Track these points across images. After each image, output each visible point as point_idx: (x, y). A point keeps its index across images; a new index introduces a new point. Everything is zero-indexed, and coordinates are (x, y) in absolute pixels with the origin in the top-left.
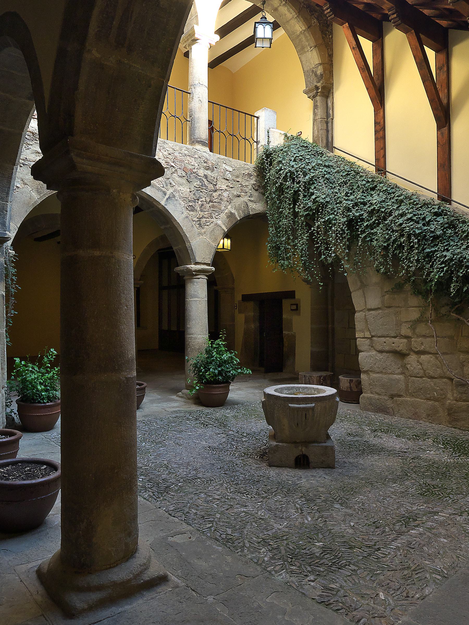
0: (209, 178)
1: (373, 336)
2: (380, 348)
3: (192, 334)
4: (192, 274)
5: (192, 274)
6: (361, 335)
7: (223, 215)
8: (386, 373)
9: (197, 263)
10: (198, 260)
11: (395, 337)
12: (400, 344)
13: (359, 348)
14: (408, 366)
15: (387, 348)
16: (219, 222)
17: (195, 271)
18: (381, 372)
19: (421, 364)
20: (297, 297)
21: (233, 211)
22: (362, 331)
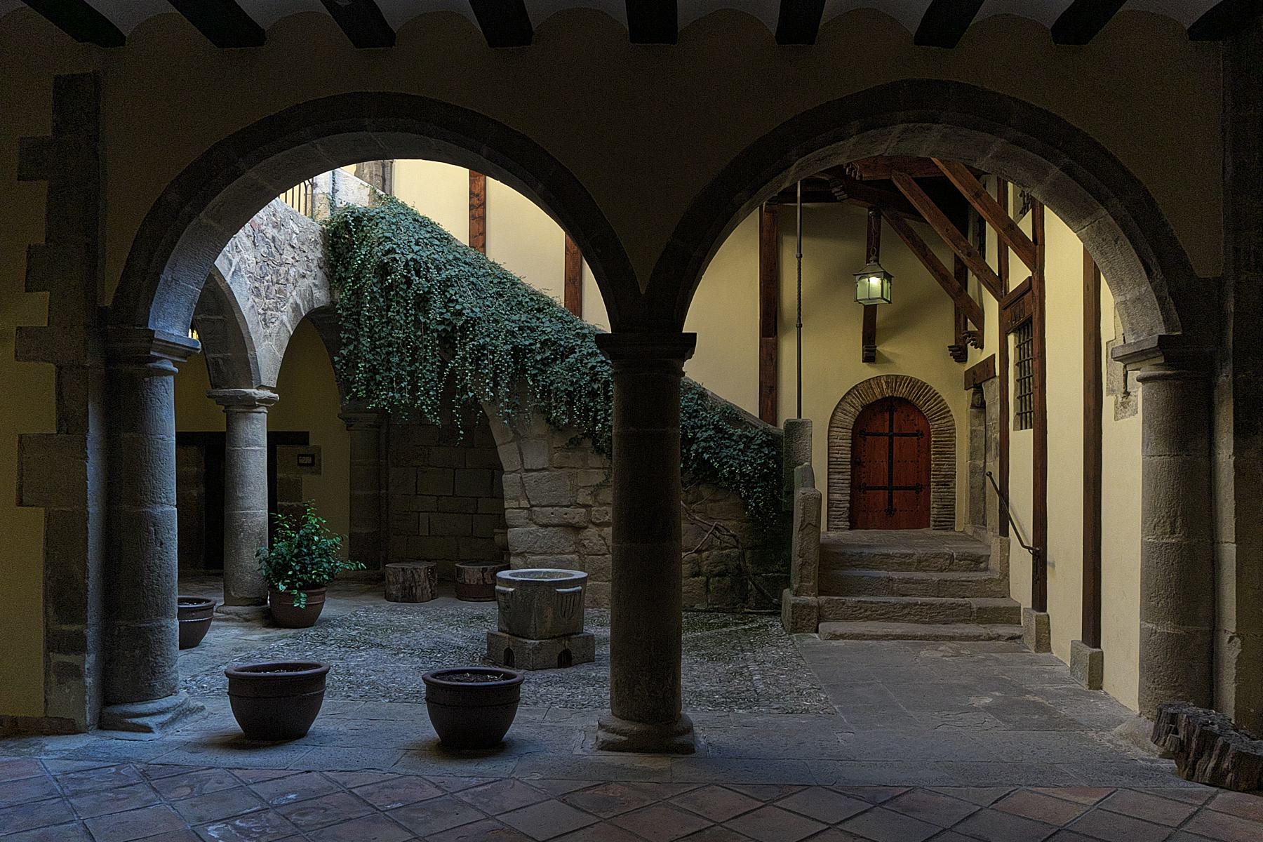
0: (278, 243)
1: (532, 506)
2: (545, 521)
3: (249, 508)
4: (250, 404)
5: (250, 404)
6: (515, 504)
7: (288, 305)
8: (551, 554)
9: (261, 387)
10: (264, 382)
11: (568, 506)
12: (577, 515)
13: (509, 523)
14: (586, 542)
15: (556, 521)
16: (285, 318)
17: (261, 400)
18: (545, 553)
19: (604, 539)
20: (312, 443)
21: (299, 301)
22: (516, 499)
